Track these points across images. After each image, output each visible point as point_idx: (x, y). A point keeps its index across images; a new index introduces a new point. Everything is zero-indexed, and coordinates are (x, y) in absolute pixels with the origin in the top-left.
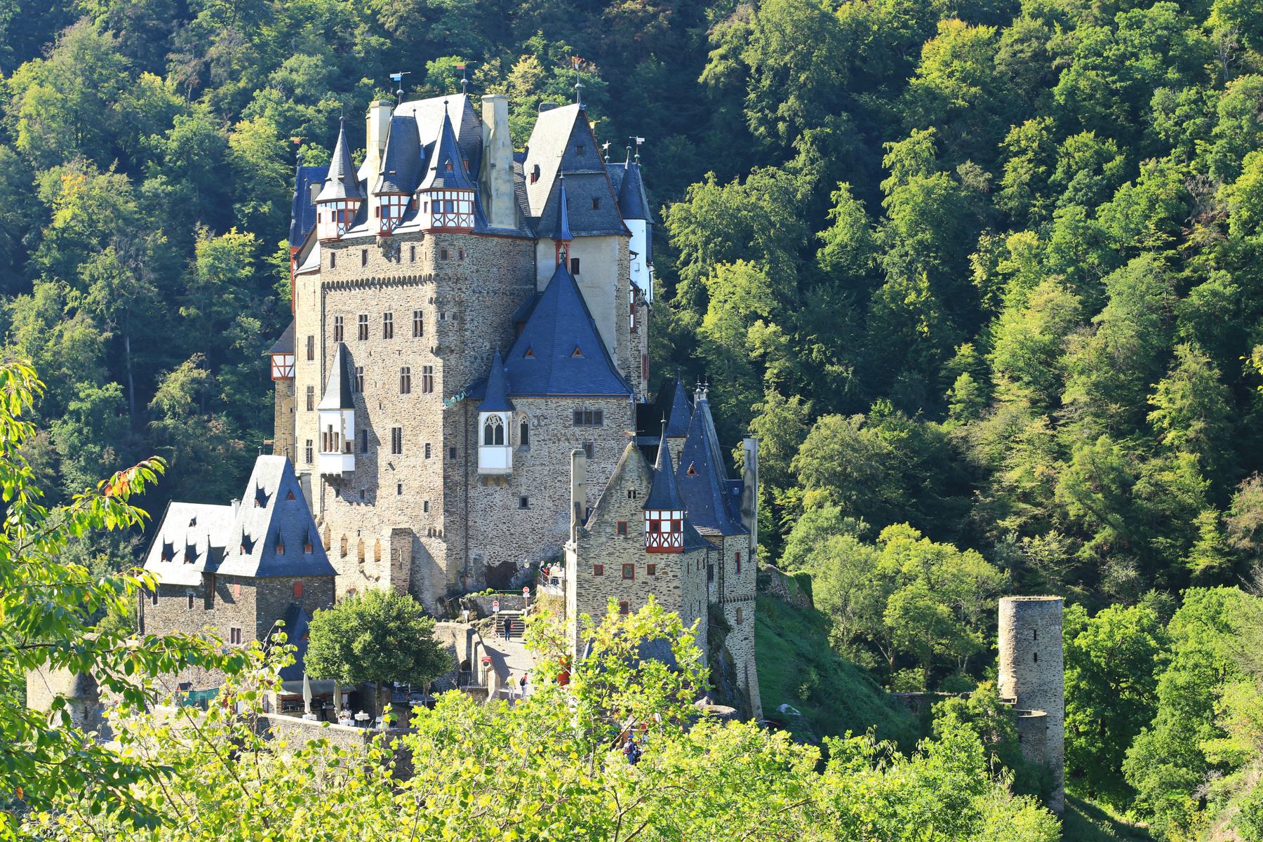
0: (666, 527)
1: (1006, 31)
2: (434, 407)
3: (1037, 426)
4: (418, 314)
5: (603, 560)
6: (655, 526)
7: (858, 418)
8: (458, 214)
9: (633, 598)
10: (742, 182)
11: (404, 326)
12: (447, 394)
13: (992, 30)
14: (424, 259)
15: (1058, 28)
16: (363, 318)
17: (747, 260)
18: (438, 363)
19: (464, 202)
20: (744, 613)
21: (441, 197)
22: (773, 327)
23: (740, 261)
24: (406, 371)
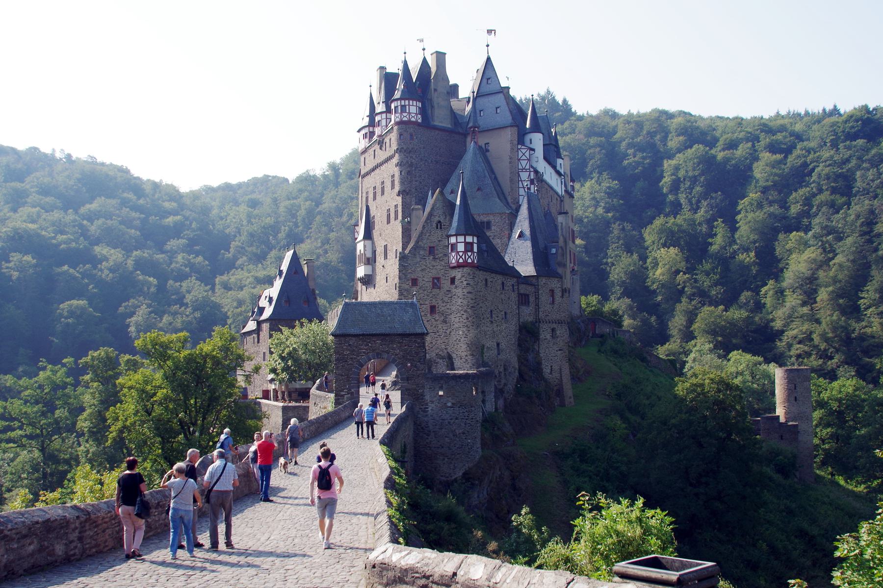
0: (461, 247)
1: (789, 156)
2: (397, 228)
3: (805, 310)
4: (393, 176)
5: (418, 274)
6: (454, 247)
7: (721, 307)
8: (409, 113)
9: (440, 302)
10: (675, 218)
11: (388, 185)
12: (403, 218)
13: (782, 156)
14: (392, 141)
15: (812, 153)
16: (375, 188)
17: (674, 247)
18: (400, 199)
19: (414, 108)
20: (558, 332)
21: (399, 104)
22: (687, 276)
23: (672, 248)
24: (389, 210)
